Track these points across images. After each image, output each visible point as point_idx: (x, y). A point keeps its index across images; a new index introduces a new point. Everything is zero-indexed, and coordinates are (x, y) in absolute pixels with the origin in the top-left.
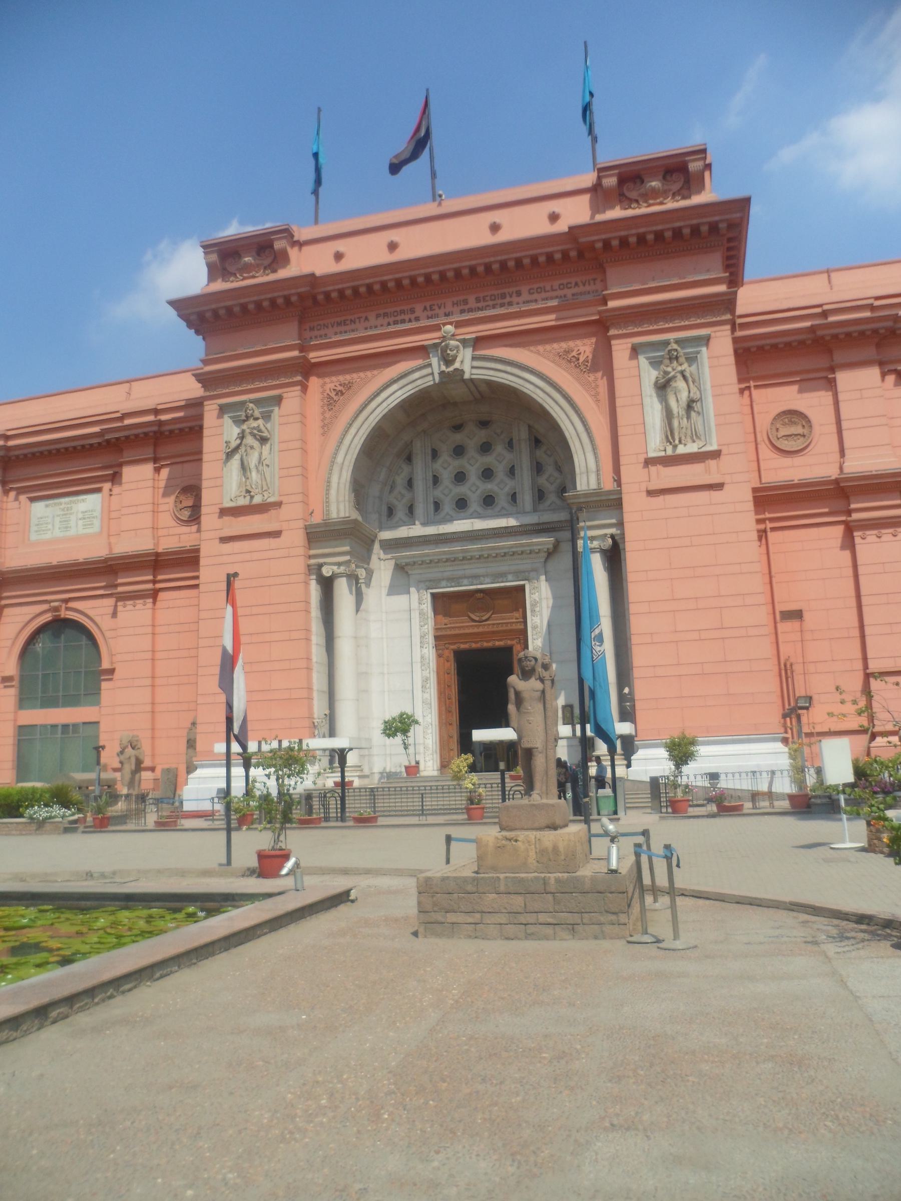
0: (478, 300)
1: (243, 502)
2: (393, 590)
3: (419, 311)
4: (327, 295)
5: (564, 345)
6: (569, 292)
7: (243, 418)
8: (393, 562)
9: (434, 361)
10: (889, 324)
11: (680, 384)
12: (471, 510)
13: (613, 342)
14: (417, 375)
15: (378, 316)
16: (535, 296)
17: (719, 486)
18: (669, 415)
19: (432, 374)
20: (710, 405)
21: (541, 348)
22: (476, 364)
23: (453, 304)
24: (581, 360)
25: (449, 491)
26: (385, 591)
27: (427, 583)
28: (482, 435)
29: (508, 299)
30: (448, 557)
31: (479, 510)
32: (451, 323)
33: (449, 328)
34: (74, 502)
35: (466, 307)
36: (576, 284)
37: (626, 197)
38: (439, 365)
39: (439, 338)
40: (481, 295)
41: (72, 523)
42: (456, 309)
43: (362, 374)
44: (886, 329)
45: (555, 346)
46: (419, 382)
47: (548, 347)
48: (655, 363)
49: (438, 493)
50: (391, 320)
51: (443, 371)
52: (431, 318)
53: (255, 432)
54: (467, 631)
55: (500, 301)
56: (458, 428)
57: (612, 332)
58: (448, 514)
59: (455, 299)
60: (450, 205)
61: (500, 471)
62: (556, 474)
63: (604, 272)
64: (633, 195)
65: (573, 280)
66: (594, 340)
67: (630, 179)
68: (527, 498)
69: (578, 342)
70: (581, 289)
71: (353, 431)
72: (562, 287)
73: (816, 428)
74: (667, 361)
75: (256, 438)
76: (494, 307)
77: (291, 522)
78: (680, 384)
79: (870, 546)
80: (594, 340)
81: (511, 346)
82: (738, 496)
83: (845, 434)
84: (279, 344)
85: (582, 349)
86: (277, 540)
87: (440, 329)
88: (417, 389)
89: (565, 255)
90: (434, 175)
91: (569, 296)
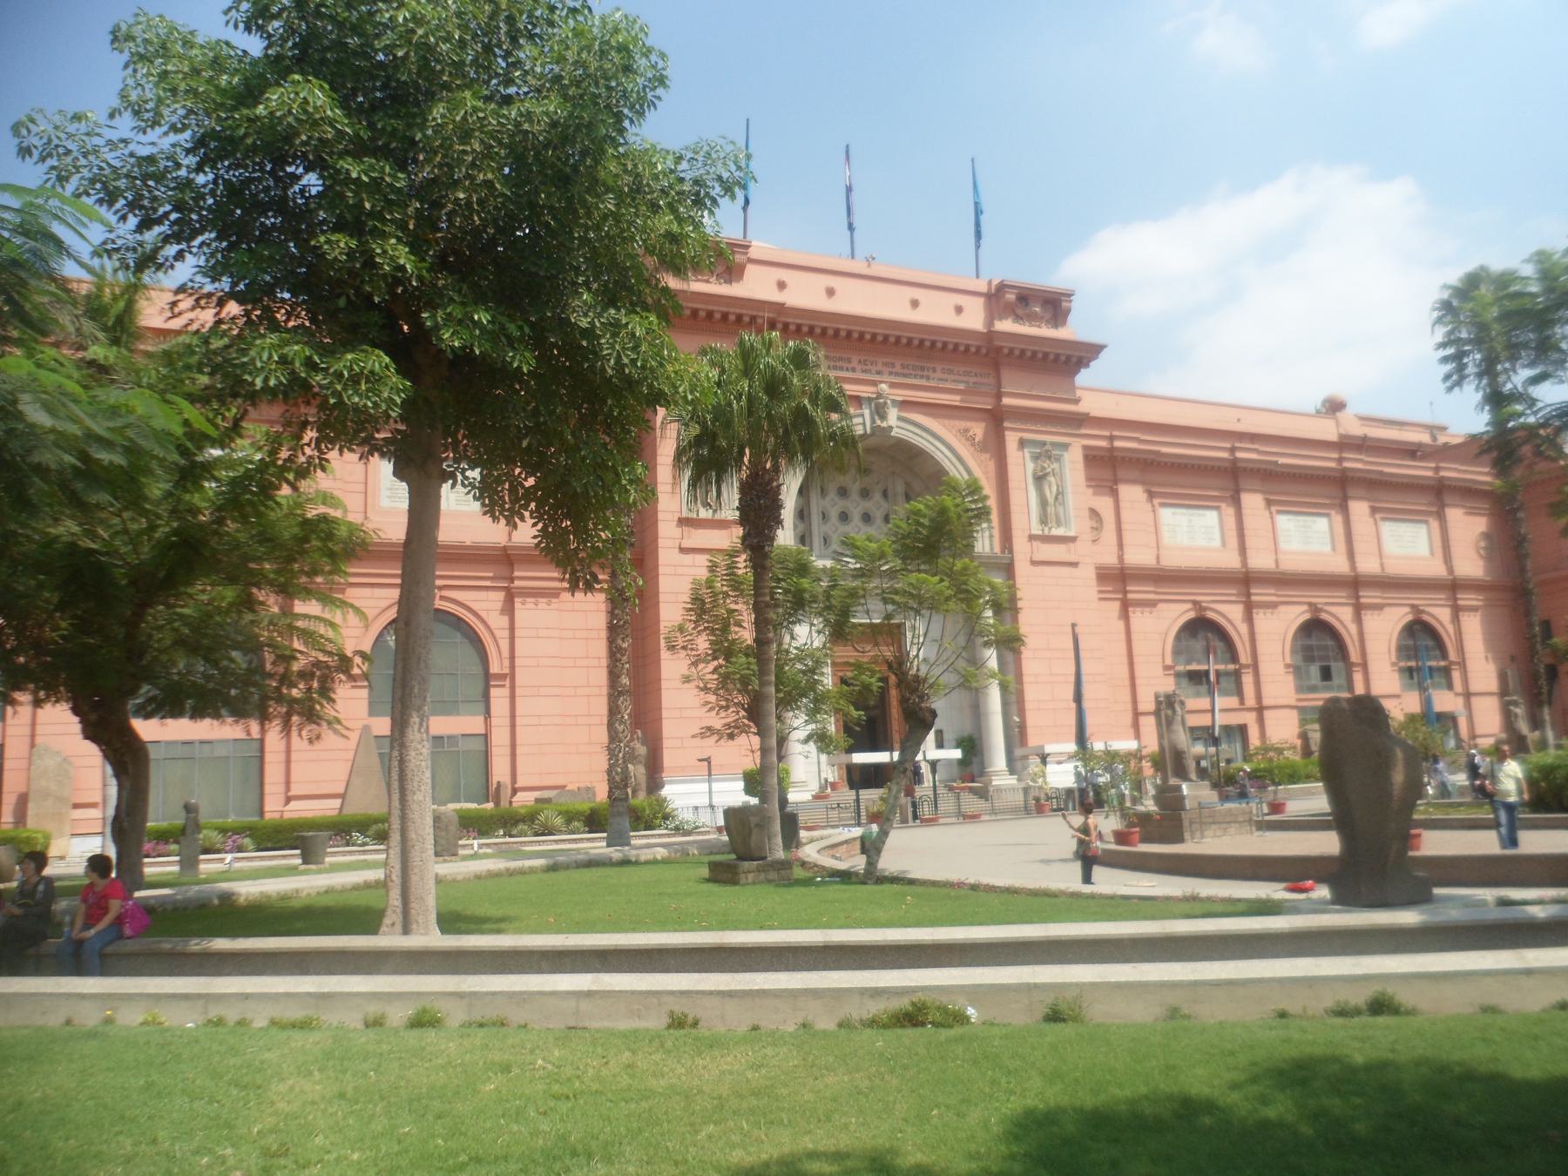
0: (903, 366)
3: (855, 363)
9: (867, 412)
11: (1052, 479)
17: (1074, 565)
18: (1043, 503)
20: (1070, 499)
21: (947, 422)
33: (884, 386)
38: (873, 421)
42: (886, 370)
47: (953, 422)
48: (1036, 458)
57: (1006, 424)
60: (876, 270)
61: (878, 515)
64: (1020, 312)
66: (983, 425)
70: (979, 379)
72: (967, 374)
78: (1052, 479)
79: (1139, 618)
82: (1087, 573)
89: (978, 349)
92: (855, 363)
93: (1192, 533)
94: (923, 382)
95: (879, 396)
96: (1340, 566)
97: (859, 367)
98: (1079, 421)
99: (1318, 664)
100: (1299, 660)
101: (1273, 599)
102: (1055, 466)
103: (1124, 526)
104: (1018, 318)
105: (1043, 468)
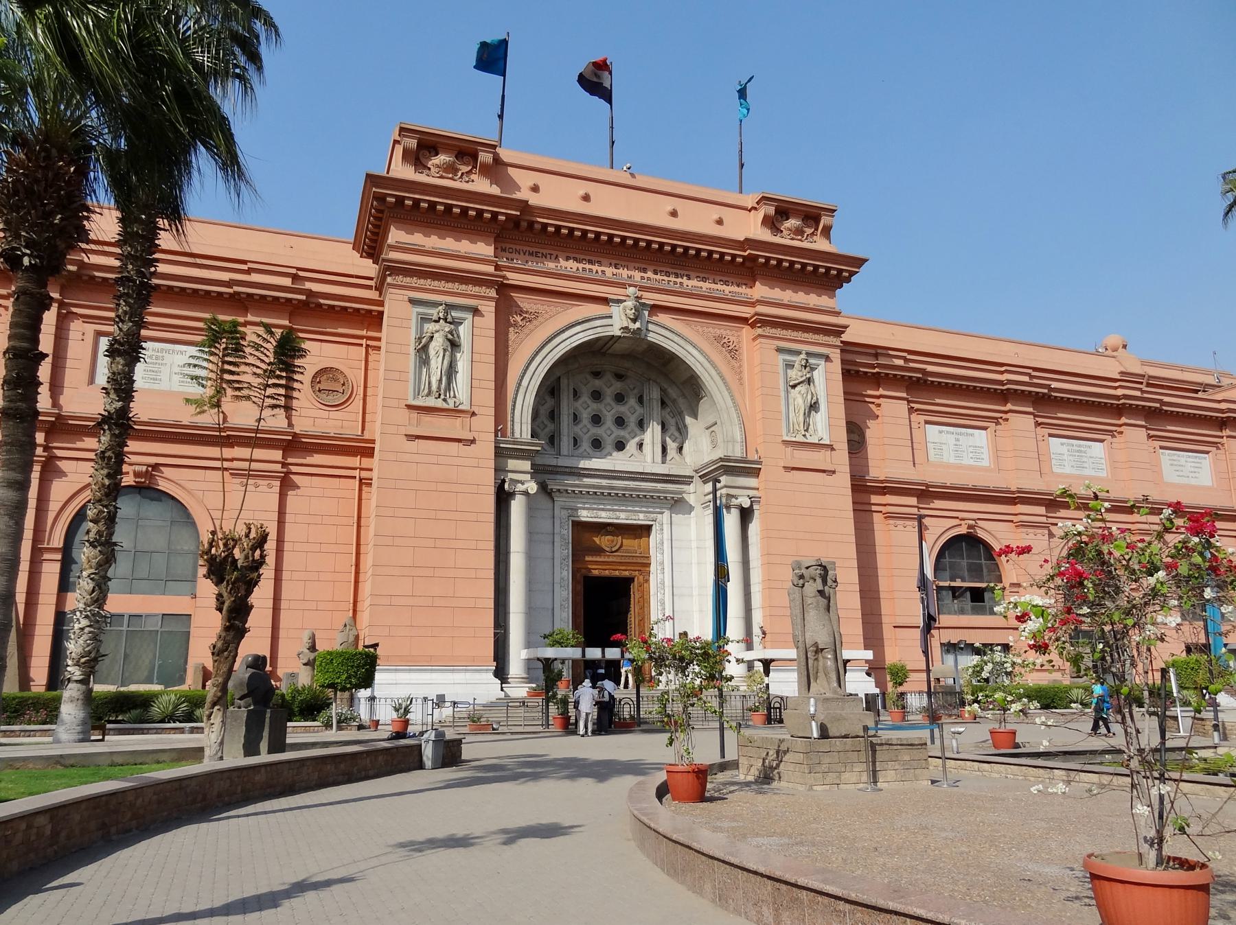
1: (431, 402)
4: (531, 224)
6: (727, 289)
7: (435, 317)
14: (598, 323)
15: (568, 259)
25: (587, 431)
28: (618, 386)
34: (168, 351)
41: (164, 376)
44: (919, 379)
46: (599, 330)
49: (577, 429)
50: (581, 266)
51: (626, 328)
53: (450, 336)
56: (597, 375)
61: (632, 421)
62: (677, 434)
70: (735, 289)
93: (959, 450)
98: (838, 331)
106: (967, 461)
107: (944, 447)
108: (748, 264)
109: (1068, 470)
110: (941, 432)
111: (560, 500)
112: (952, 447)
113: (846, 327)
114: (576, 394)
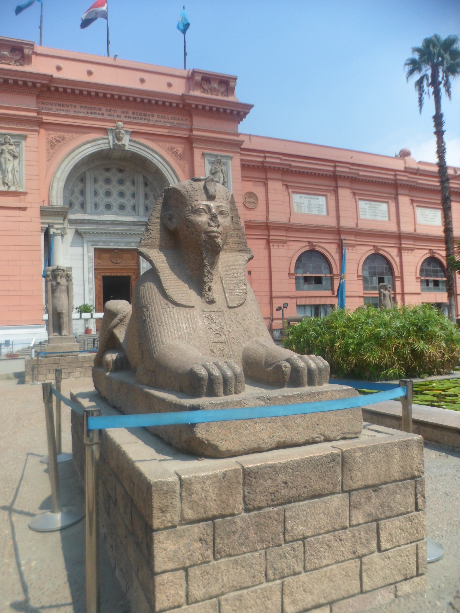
0: (133, 113)
2: (73, 244)
3: (104, 111)
5: (171, 145)
6: (175, 122)
8: (74, 230)
9: (111, 137)
10: (288, 167)
12: (113, 211)
13: (195, 150)
14: (101, 142)
16: (160, 119)
19: (109, 143)
21: (161, 144)
22: (131, 143)
23: (121, 112)
24: (178, 153)
25: (102, 200)
26: (69, 244)
27: (92, 243)
28: (120, 176)
29: (147, 117)
30: (105, 231)
31: (118, 211)
32: (121, 121)
33: (120, 123)
35: (127, 115)
36: (179, 119)
37: (202, 87)
38: (114, 141)
39: (114, 127)
40: (135, 111)
42: (123, 115)
43: (70, 134)
45: (167, 144)
46: (102, 146)
47: (164, 144)
48: (211, 163)
49: (97, 200)
51: (116, 144)
52: (110, 115)
54: (110, 267)
55: (144, 117)
56: (107, 170)
57: (194, 145)
58: (102, 211)
59: (122, 110)
61: (128, 194)
63: (191, 117)
65: (178, 117)
67: (206, 79)
68: (142, 209)
69: (177, 145)
71: (66, 162)
72: (172, 118)
73: (259, 201)
74: (216, 163)
75: (11, 156)
76: (141, 119)
77: (34, 203)
80: (183, 146)
81: (147, 139)
83: (270, 206)
84: (26, 106)
85: (179, 149)
86: (24, 212)
87: (115, 123)
88: (100, 149)
89: (178, 105)
90: (108, 42)
91: (175, 124)
92: (104, 111)
94: (146, 122)
95: (117, 127)
96: (392, 228)
97: (106, 113)
99: (377, 276)
100: (366, 274)
101: (354, 242)
102: (224, 168)
103: (270, 202)
104: (204, 91)
105: (215, 168)
106: (315, 212)
107: (302, 205)
108: (186, 108)
109: (368, 217)
110: (301, 197)
111: (86, 238)
112: (307, 205)
113: (243, 142)
114: (96, 181)
